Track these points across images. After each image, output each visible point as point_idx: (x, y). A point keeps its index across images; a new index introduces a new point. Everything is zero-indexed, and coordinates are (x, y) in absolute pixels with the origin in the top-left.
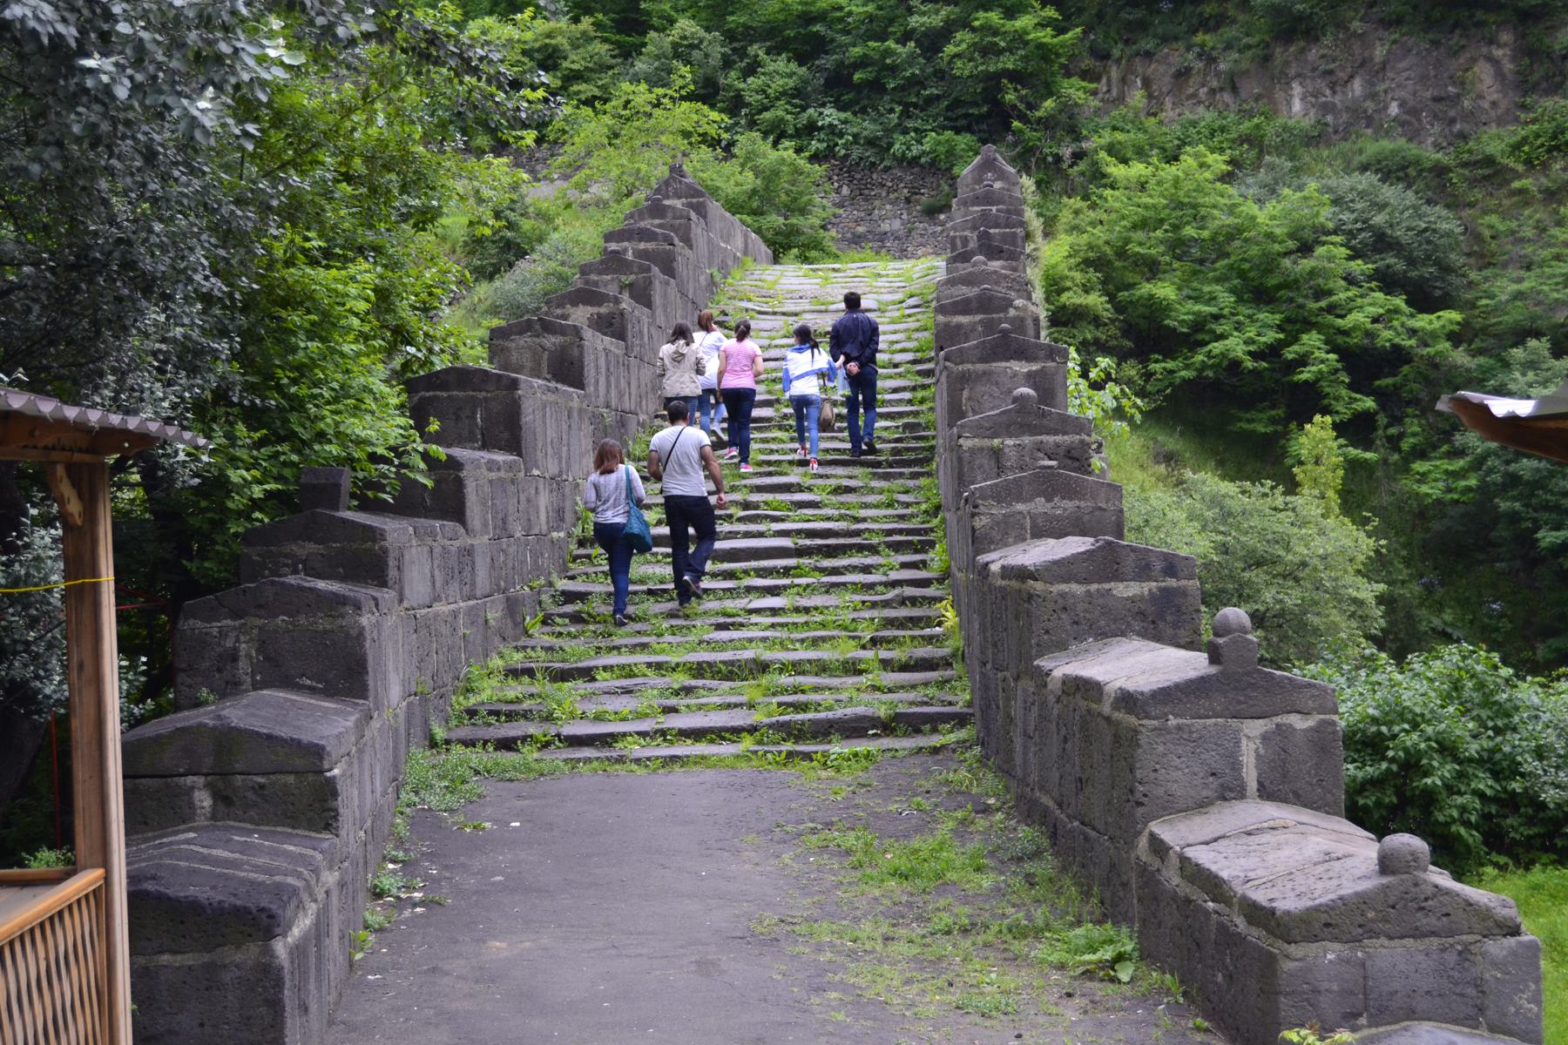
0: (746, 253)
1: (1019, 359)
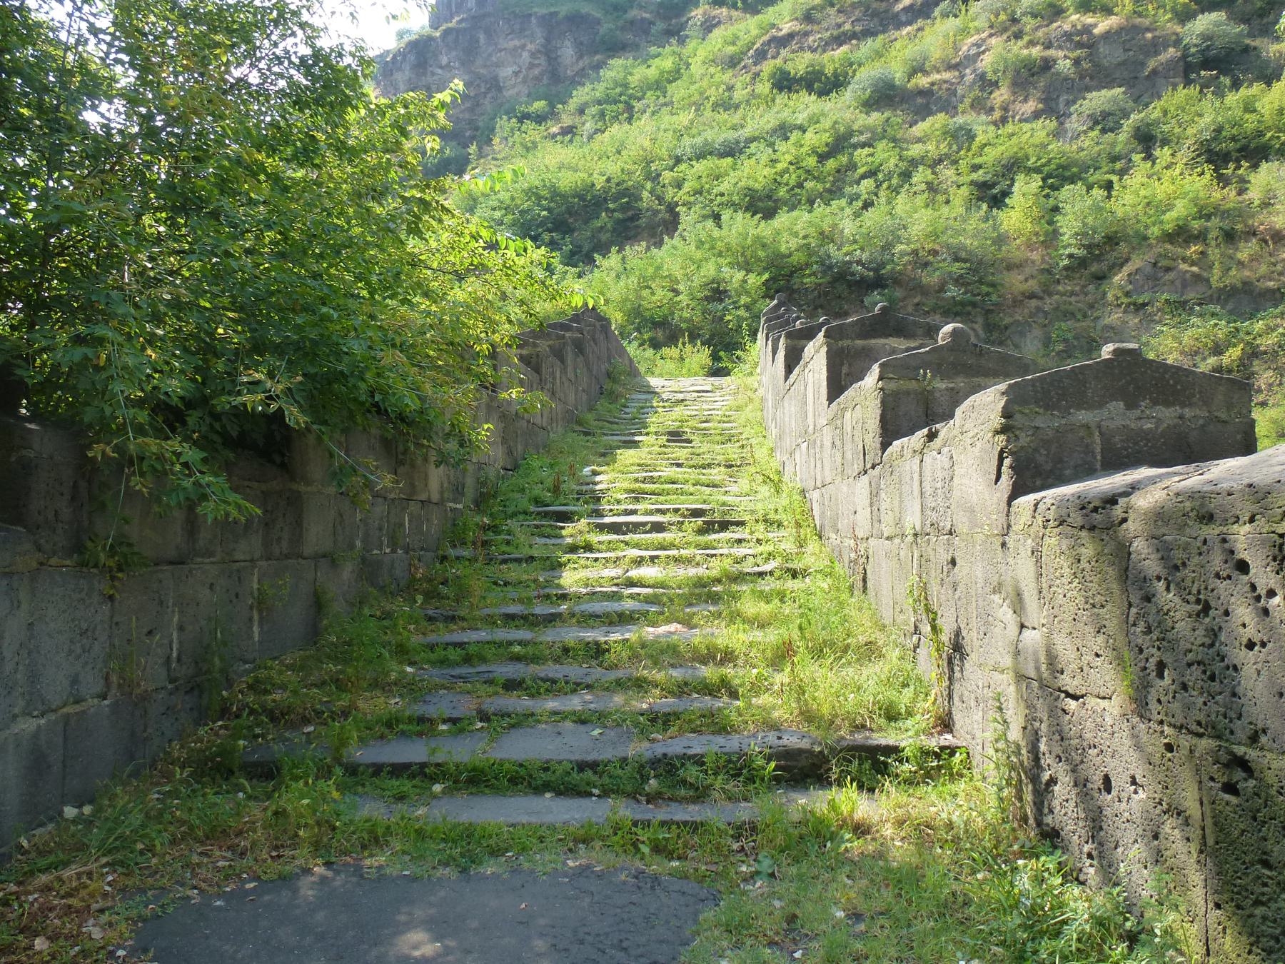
1: (899, 336)
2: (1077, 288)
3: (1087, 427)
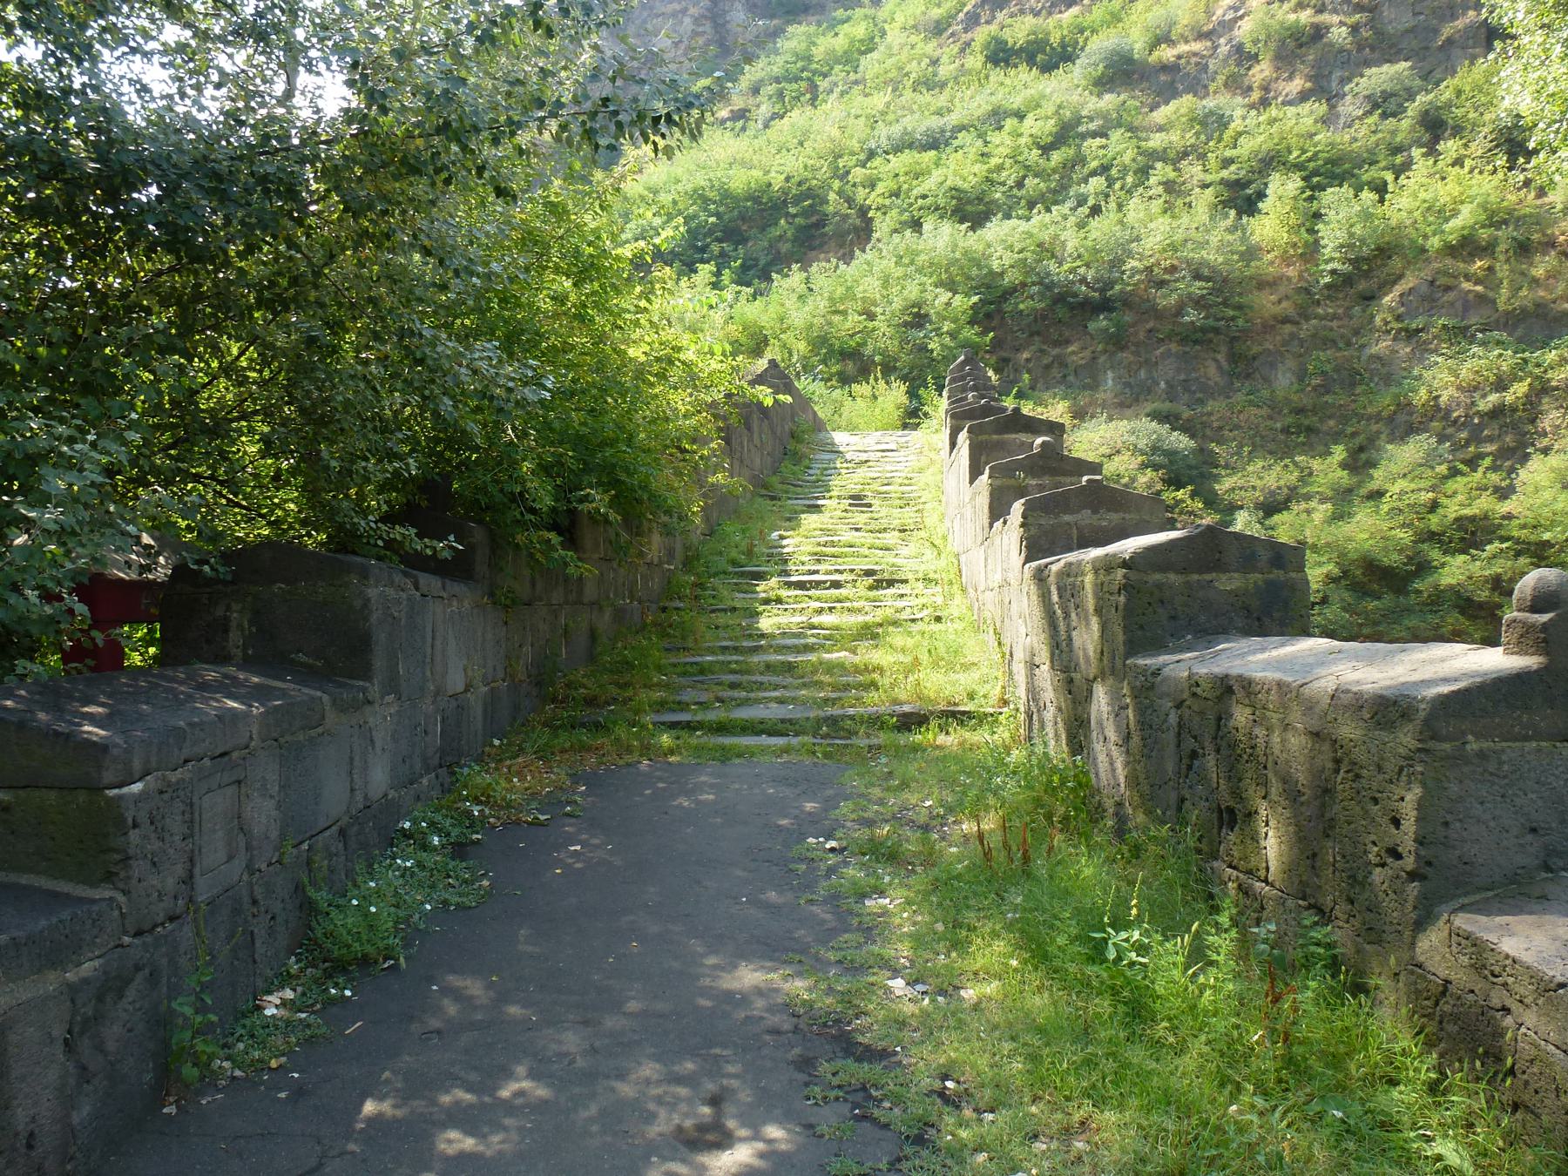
2: (1340, 311)
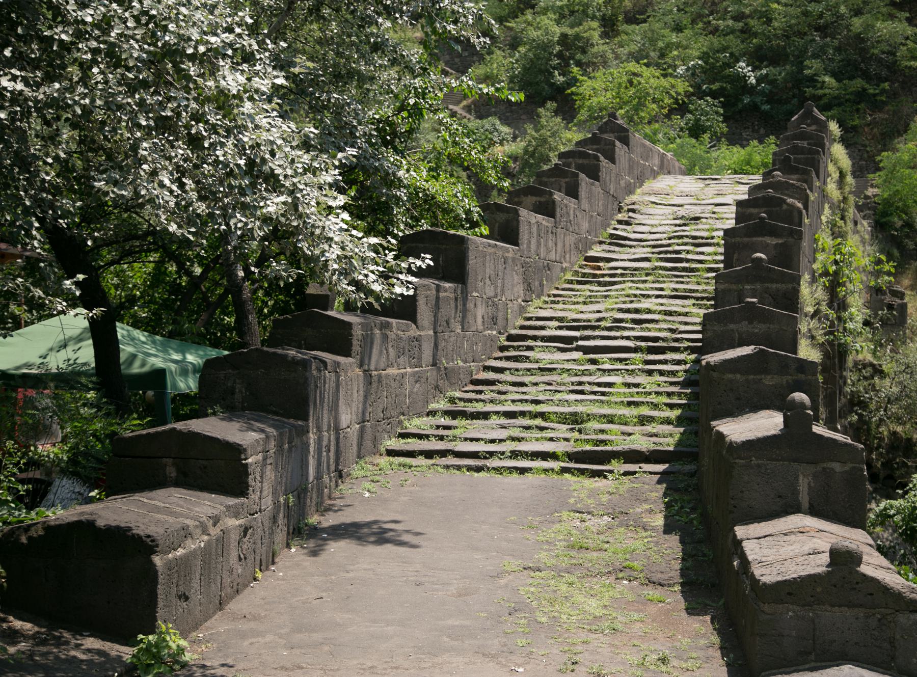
0: (662, 166)
1: (771, 236)
3: (732, 330)
